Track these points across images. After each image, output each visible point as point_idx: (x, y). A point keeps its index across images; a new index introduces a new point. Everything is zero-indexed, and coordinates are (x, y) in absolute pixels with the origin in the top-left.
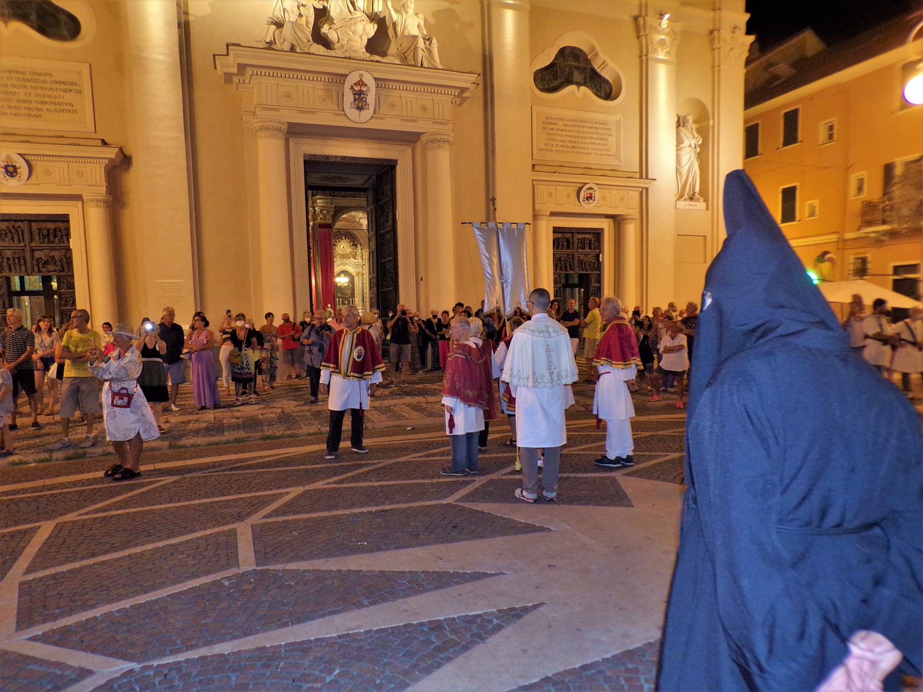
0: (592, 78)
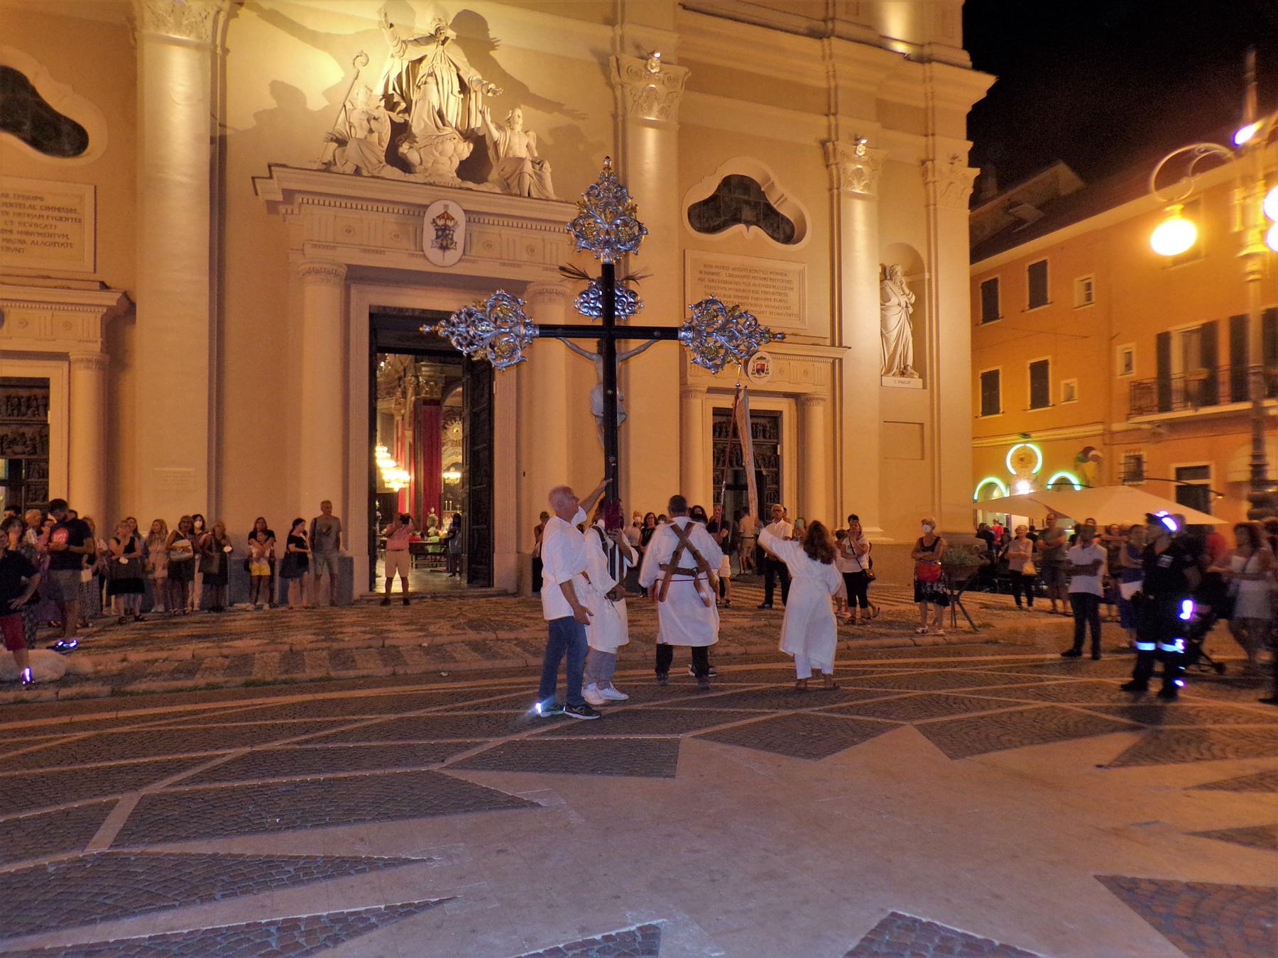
0: (766, 216)
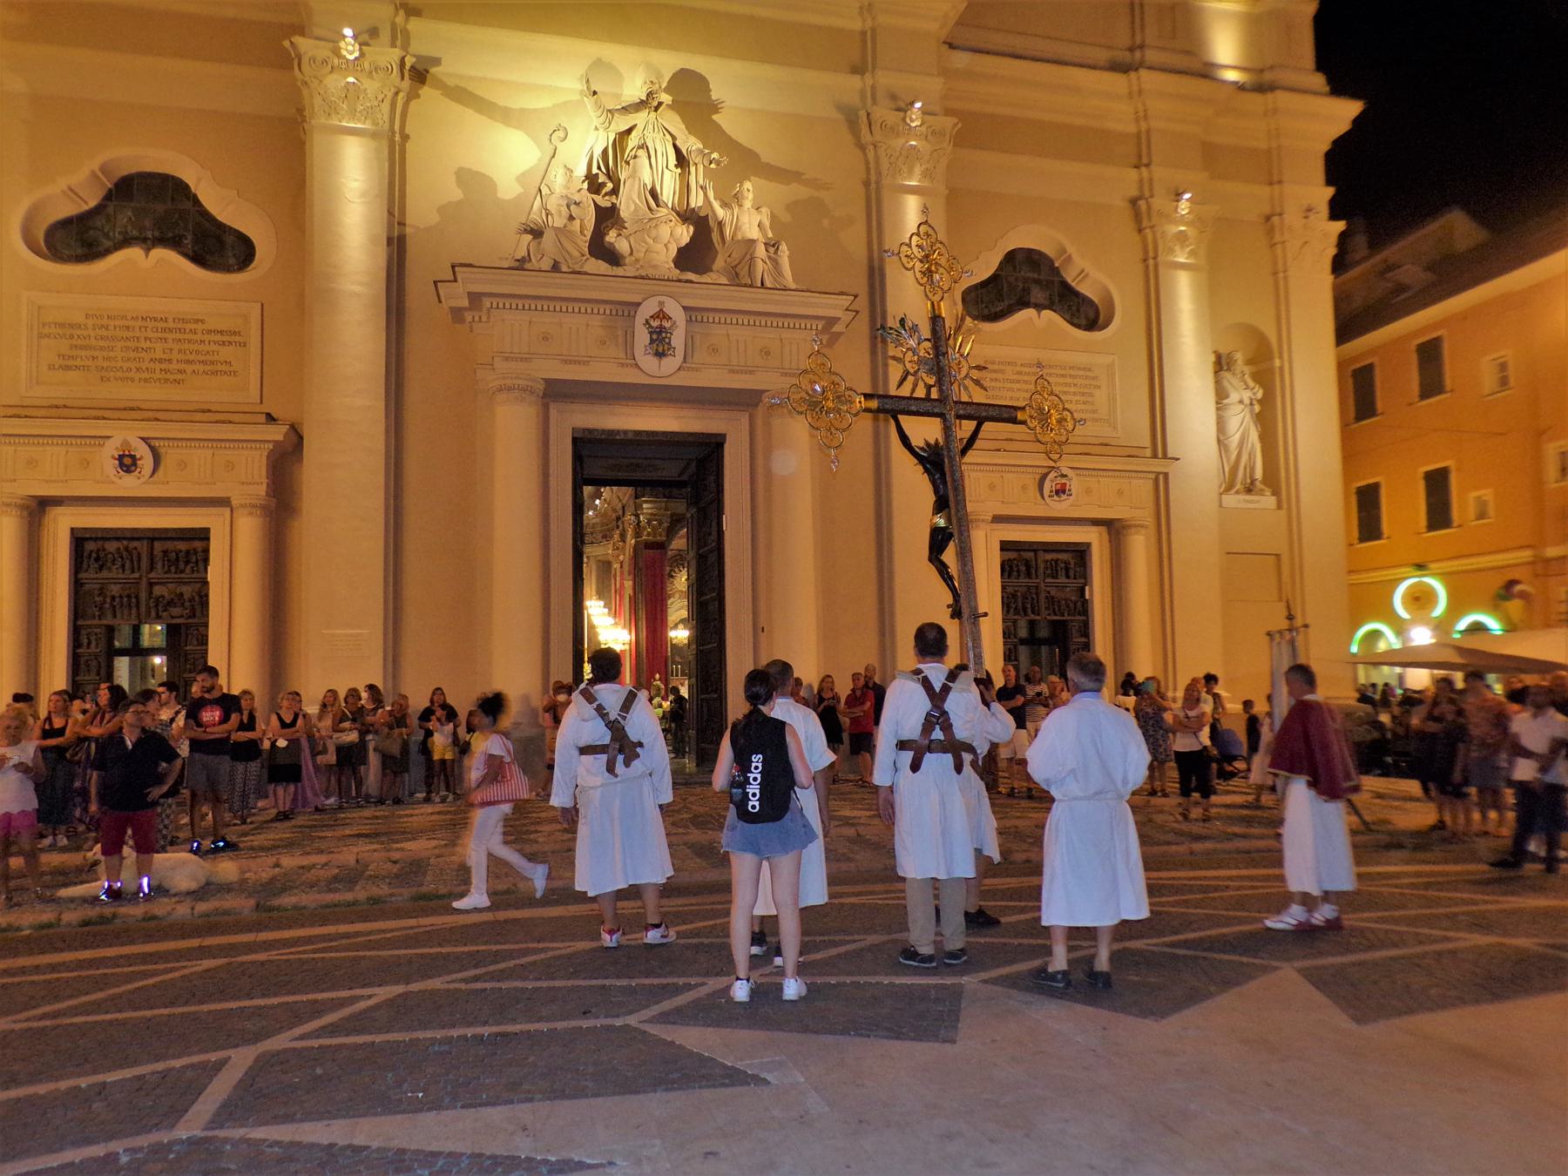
0: (1062, 297)
